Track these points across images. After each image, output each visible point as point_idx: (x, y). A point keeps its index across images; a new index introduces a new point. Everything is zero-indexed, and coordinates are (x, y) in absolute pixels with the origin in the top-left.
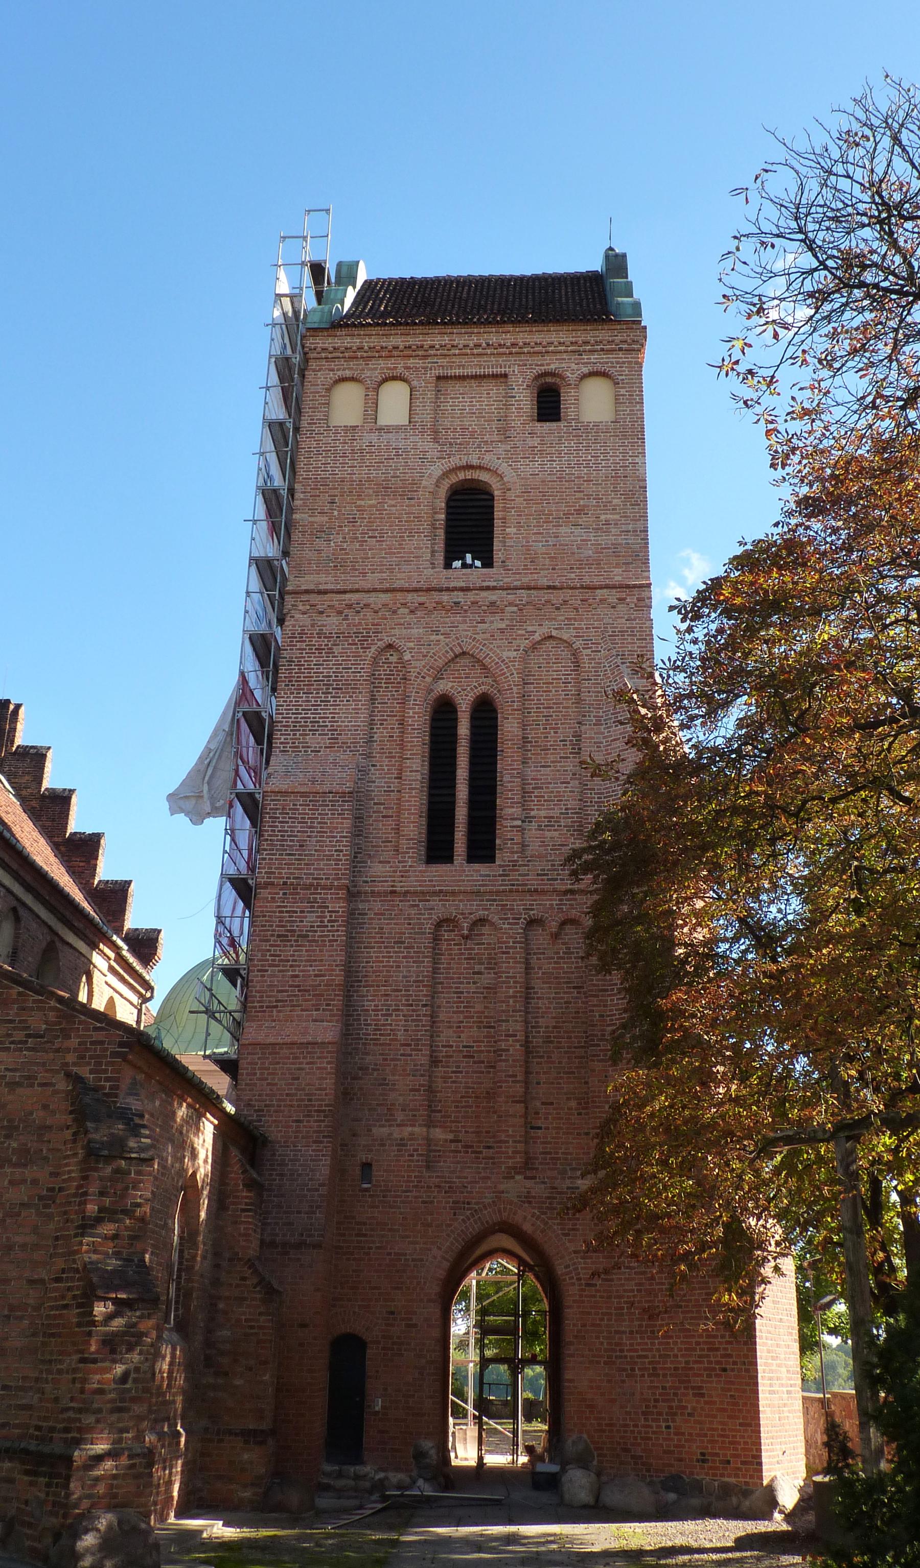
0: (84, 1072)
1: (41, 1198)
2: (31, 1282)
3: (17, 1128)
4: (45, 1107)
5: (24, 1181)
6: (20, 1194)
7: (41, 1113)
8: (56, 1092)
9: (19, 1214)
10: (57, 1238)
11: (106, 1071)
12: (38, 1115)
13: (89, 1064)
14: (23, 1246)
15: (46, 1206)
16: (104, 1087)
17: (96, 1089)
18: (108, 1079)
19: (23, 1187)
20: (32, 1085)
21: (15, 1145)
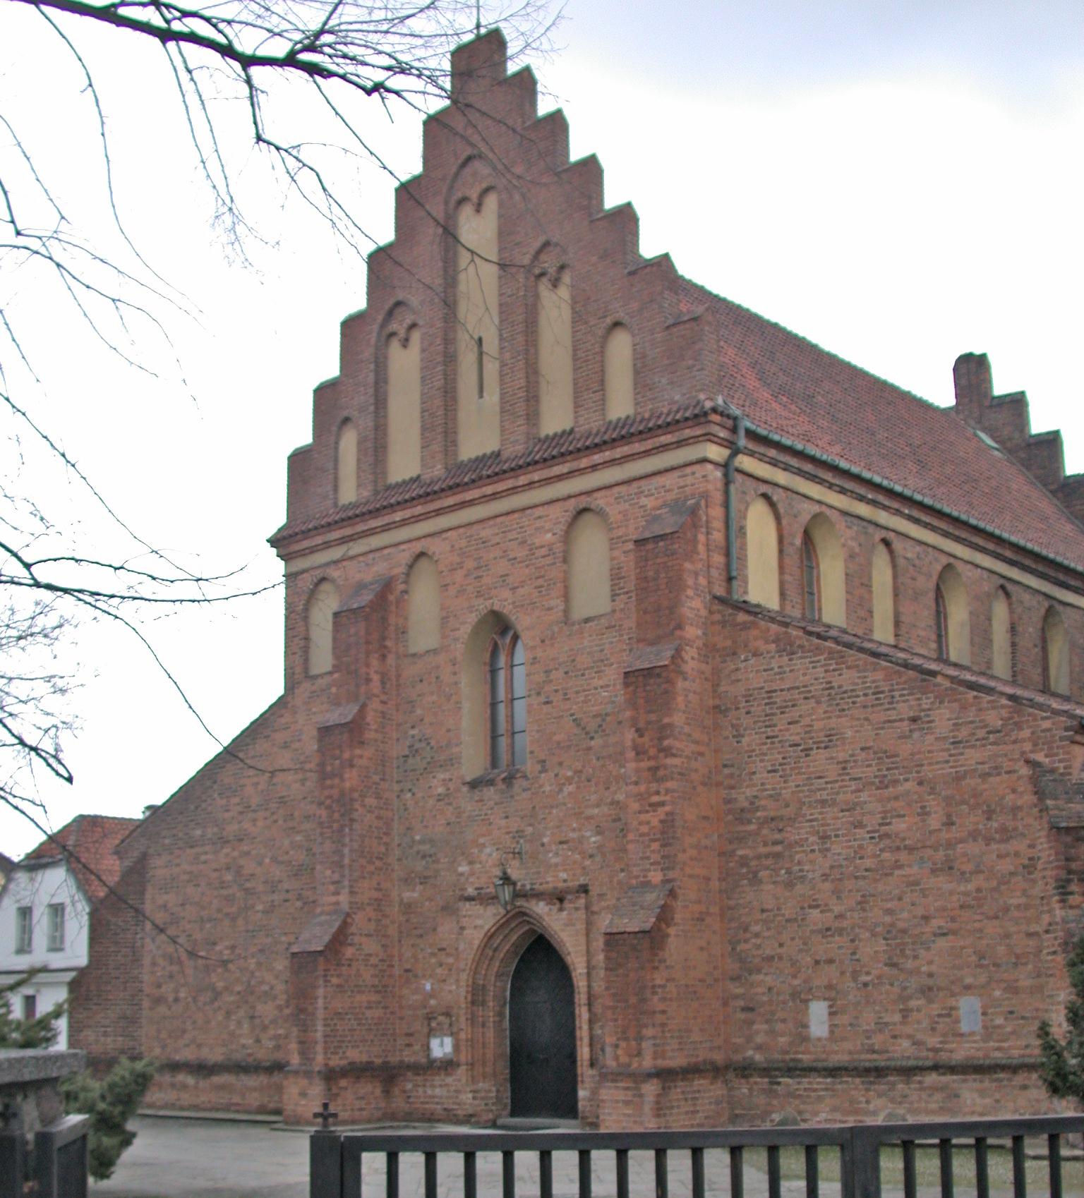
0: (1040, 757)
1: (1024, 867)
2: (1030, 935)
3: (993, 811)
4: (1014, 791)
5: (1007, 855)
6: (1006, 866)
7: (1012, 796)
8: (1019, 778)
9: (1009, 882)
10: (1042, 898)
11: (1057, 755)
12: (1010, 798)
13: (1042, 750)
14: (1018, 907)
15: (1030, 873)
16: (1058, 768)
17: (1053, 771)
18: (1060, 761)
19: (1008, 860)
20: (999, 774)
21: (995, 825)
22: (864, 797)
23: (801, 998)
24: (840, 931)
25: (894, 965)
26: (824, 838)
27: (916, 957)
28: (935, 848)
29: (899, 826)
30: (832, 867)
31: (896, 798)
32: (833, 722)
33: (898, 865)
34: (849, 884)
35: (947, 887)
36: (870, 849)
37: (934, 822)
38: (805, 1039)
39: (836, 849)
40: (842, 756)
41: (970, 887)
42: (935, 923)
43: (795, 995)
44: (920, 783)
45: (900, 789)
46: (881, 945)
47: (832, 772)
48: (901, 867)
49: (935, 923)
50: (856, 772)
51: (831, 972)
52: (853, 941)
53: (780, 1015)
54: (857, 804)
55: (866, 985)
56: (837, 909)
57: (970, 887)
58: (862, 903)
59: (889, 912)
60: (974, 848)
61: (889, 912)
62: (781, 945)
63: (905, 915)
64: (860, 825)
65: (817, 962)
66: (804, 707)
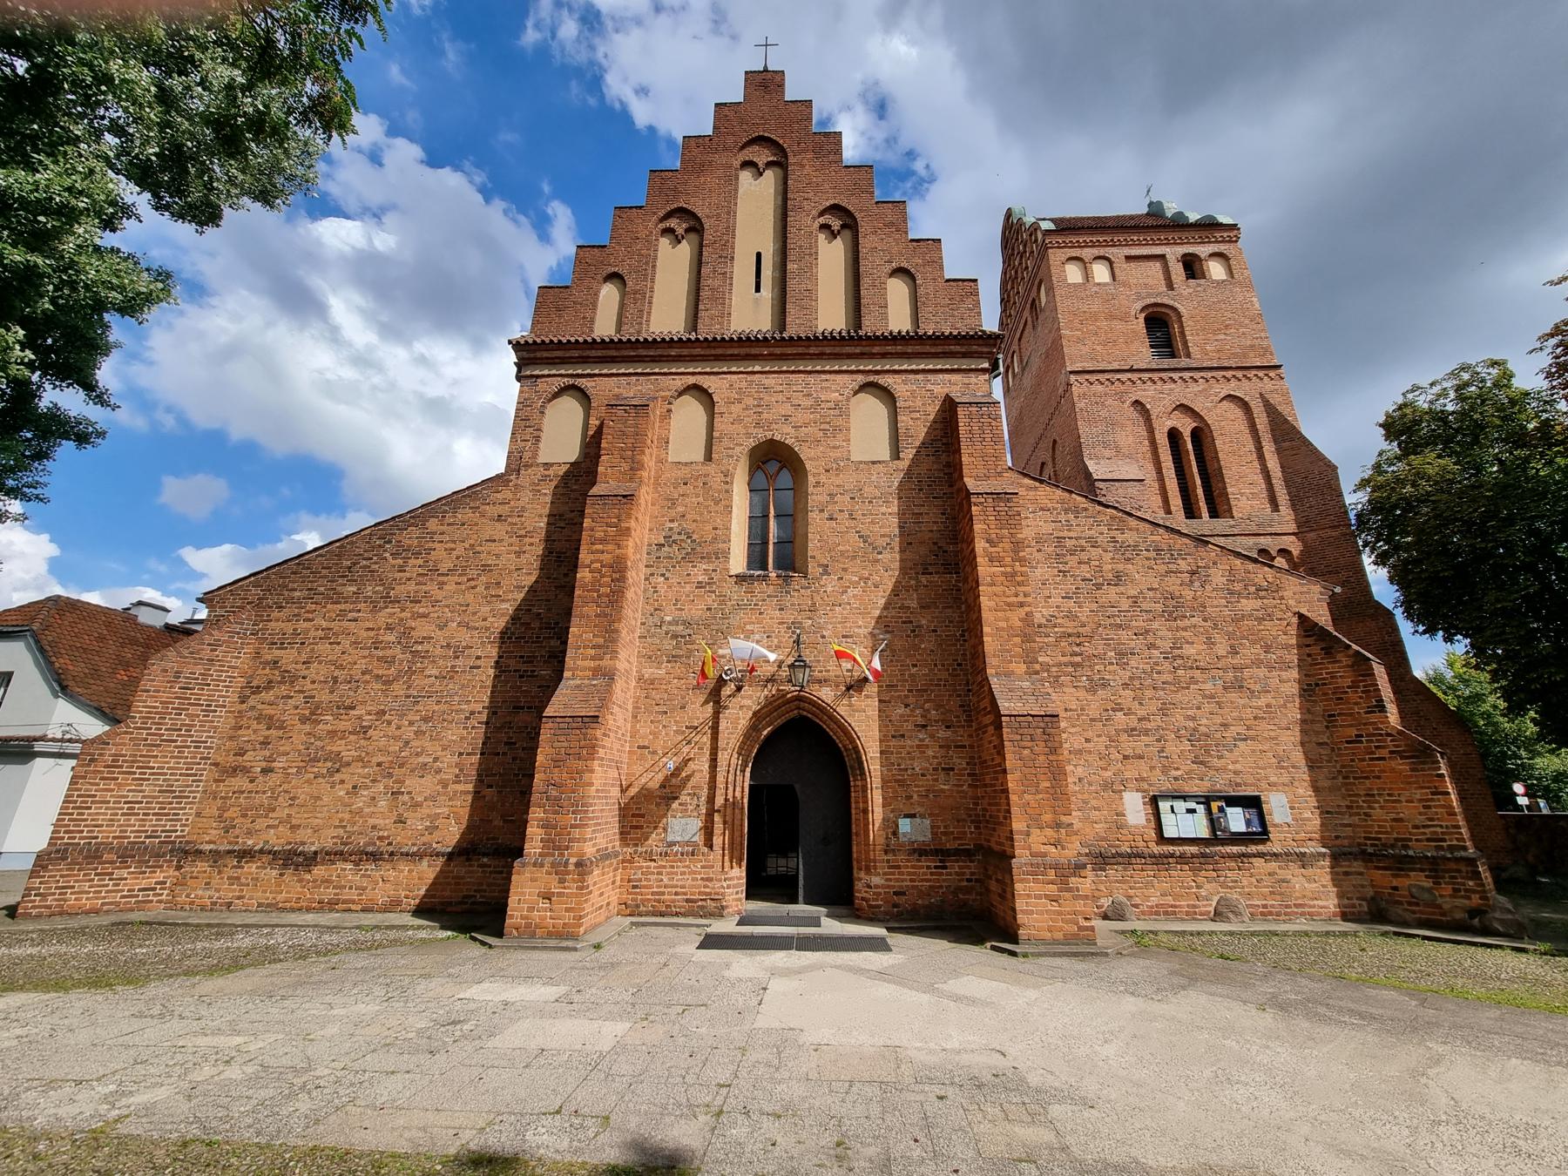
22: (1155, 625)
23: (1114, 788)
24: (1146, 732)
25: (1201, 763)
26: (1121, 654)
27: (1220, 757)
28: (1224, 670)
29: (1189, 650)
30: (1131, 678)
31: (1185, 629)
32: (1120, 567)
33: (1193, 680)
34: (1149, 693)
35: (1242, 702)
36: (1167, 666)
37: (1221, 649)
38: (1120, 827)
39: (1133, 663)
40: (1133, 592)
41: (1262, 702)
42: (1234, 730)
43: (1107, 785)
44: (1205, 620)
45: (1187, 622)
46: (1187, 745)
47: (1125, 604)
48: (1196, 683)
49: (1234, 730)
50: (1145, 606)
51: (1142, 768)
52: (1158, 740)
53: (1094, 803)
54: (1147, 632)
55: (1176, 779)
56: (1141, 713)
57: (1262, 702)
58: (1164, 711)
59: (1193, 719)
60: (1261, 672)
61: (1193, 719)
62: (1087, 741)
63: (1204, 721)
64: (1151, 646)
65: (1126, 757)
66: (1095, 552)
